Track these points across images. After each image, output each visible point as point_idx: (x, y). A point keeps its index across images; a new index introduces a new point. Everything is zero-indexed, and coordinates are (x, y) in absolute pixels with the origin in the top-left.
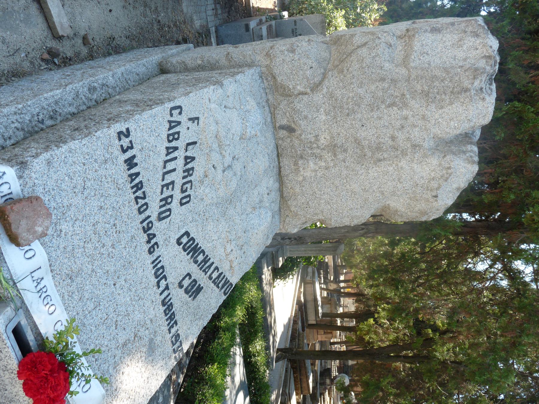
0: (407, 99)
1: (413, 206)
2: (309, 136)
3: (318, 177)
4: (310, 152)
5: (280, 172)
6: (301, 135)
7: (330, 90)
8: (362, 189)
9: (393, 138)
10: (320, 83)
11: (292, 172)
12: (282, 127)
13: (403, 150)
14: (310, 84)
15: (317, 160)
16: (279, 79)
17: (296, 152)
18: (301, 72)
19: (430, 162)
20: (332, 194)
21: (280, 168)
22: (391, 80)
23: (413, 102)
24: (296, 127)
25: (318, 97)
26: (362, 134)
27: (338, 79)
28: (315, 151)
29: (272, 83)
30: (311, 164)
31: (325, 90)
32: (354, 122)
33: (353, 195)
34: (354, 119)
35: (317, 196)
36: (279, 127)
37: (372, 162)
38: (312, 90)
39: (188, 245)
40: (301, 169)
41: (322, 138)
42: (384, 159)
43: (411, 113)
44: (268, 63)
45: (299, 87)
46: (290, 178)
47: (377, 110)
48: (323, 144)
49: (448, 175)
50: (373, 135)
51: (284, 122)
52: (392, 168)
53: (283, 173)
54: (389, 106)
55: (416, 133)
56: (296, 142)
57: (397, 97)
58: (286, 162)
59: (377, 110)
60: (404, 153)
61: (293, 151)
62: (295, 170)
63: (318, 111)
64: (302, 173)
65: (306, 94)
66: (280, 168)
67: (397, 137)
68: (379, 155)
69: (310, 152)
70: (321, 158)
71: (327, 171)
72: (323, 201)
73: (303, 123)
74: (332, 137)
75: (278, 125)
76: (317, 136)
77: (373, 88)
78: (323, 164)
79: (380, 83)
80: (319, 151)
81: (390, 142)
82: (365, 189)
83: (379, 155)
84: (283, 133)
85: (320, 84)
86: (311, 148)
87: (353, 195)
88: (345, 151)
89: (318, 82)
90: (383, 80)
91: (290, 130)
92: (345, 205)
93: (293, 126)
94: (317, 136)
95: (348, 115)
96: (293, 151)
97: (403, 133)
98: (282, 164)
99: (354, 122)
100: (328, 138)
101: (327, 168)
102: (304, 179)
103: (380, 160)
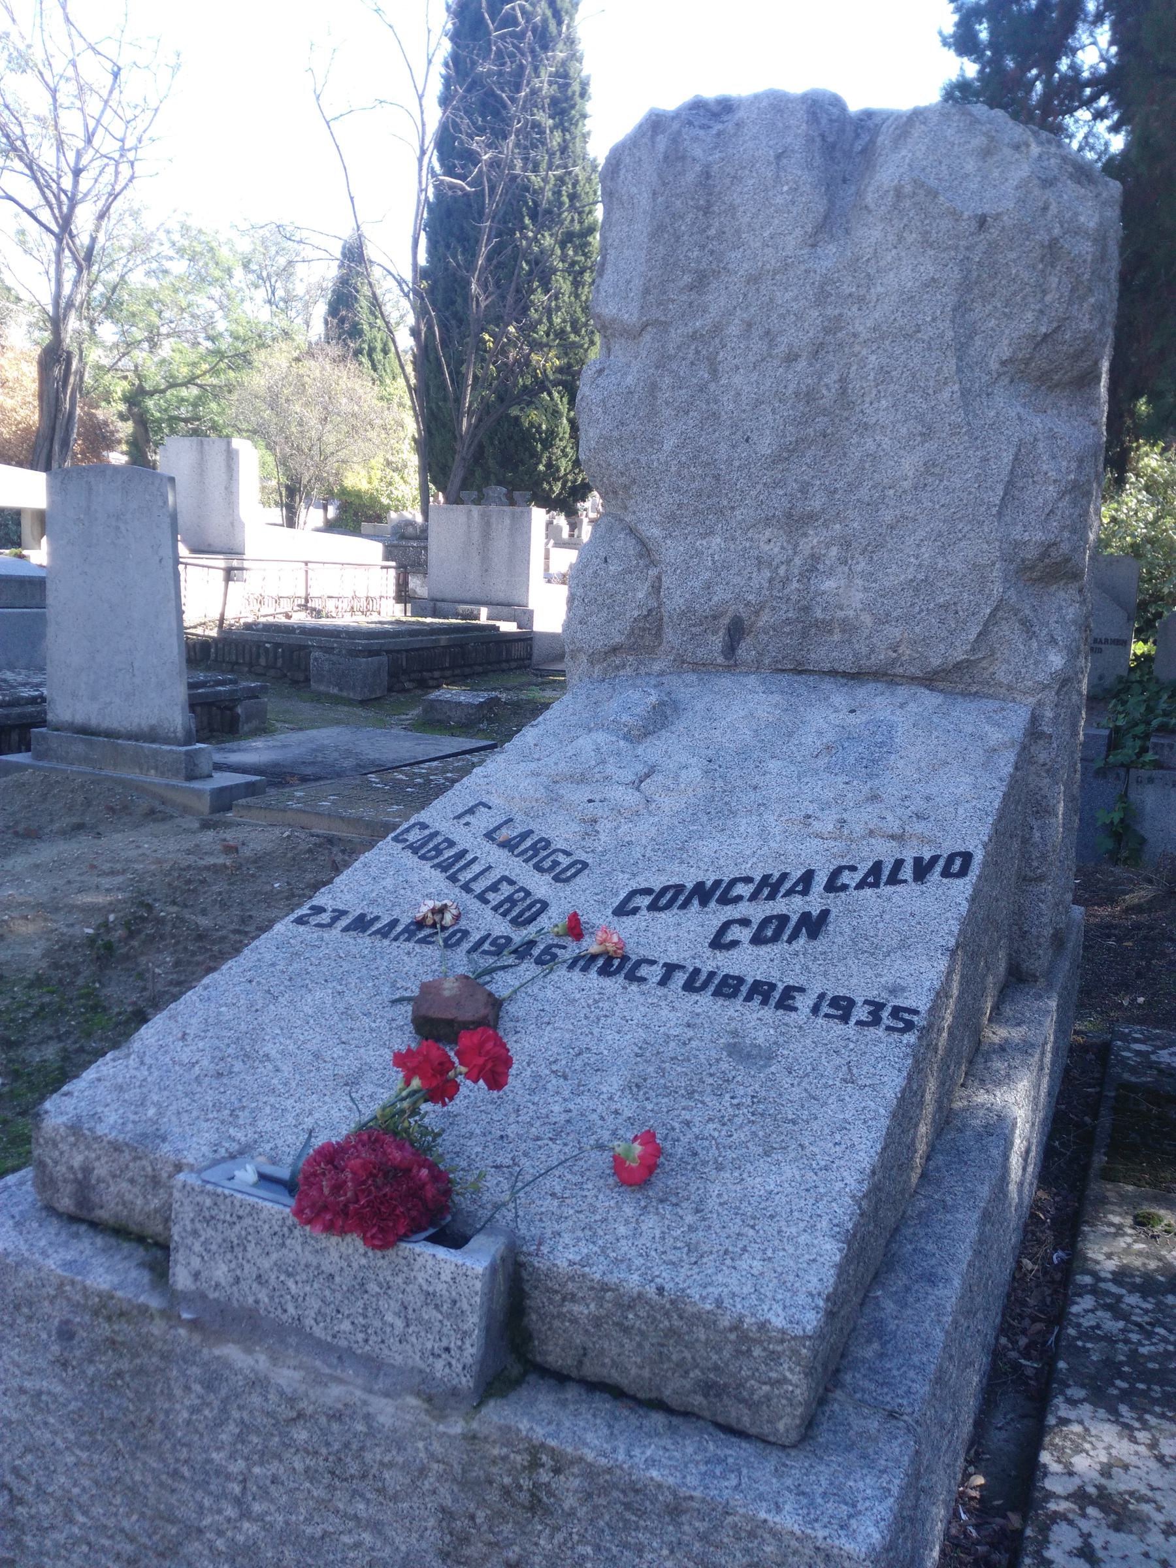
0: (703, 327)
1: (1015, 287)
2: (755, 583)
3: (869, 569)
4: (795, 585)
5: (845, 674)
6: (748, 604)
7: (658, 518)
8: (923, 443)
9: (791, 358)
10: (642, 542)
11: (849, 641)
12: (730, 649)
13: (824, 329)
14: (638, 565)
15: (821, 567)
16: (618, 639)
17: (788, 622)
18: (610, 585)
19: (870, 250)
20: (921, 534)
21: (833, 673)
22: (657, 367)
23: (714, 312)
24: (729, 614)
25: (671, 551)
26: (765, 445)
27: (639, 499)
28: (796, 572)
29: (630, 658)
30: (829, 584)
31: (656, 532)
32: (736, 463)
33: (937, 470)
34: (730, 461)
35: (921, 576)
36: (726, 658)
37: (846, 414)
38: (654, 563)
39: (527, 914)
40: (840, 614)
41: (767, 548)
42: (843, 380)
43: (738, 312)
44: (584, 658)
45: (640, 595)
46: (865, 650)
47: (716, 402)
48: (783, 548)
49: (922, 192)
50: (774, 412)
51: (717, 641)
52: (873, 357)
53: (848, 666)
54: (714, 372)
55: (788, 295)
56: (765, 618)
57: (697, 352)
58: (821, 655)
59: (716, 402)
60: (833, 326)
61: (787, 629)
62: (843, 631)
63: (699, 553)
64: (851, 613)
65: (659, 578)
66: (833, 673)
67: (790, 346)
68: (828, 397)
69: (795, 585)
70: (815, 558)
71: (854, 544)
72: (941, 562)
73: (720, 594)
74: (768, 521)
75: (720, 660)
76: (760, 562)
77: (668, 412)
78: (834, 551)
79: (659, 394)
80: (797, 561)
81: (802, 364)
82: (922, 434)
83: (828, 397)
84: (746, 651)
85: (644, 545)
86: (786, 581)
87: (937, 470)
88: (804, 489)
89: (638, 548)
90: (653, 388)
91: (736, 631)
92: (964, 495)
93: (725, 621)
94: (760, 562)
95: (717, 478)
96: (787, 629)
97: (782, 332)
98: (827, 666)
99: (736, 463)
100: (768, 533)
101: (846, 544)
102: (867, 607)
103: (843, 391)
